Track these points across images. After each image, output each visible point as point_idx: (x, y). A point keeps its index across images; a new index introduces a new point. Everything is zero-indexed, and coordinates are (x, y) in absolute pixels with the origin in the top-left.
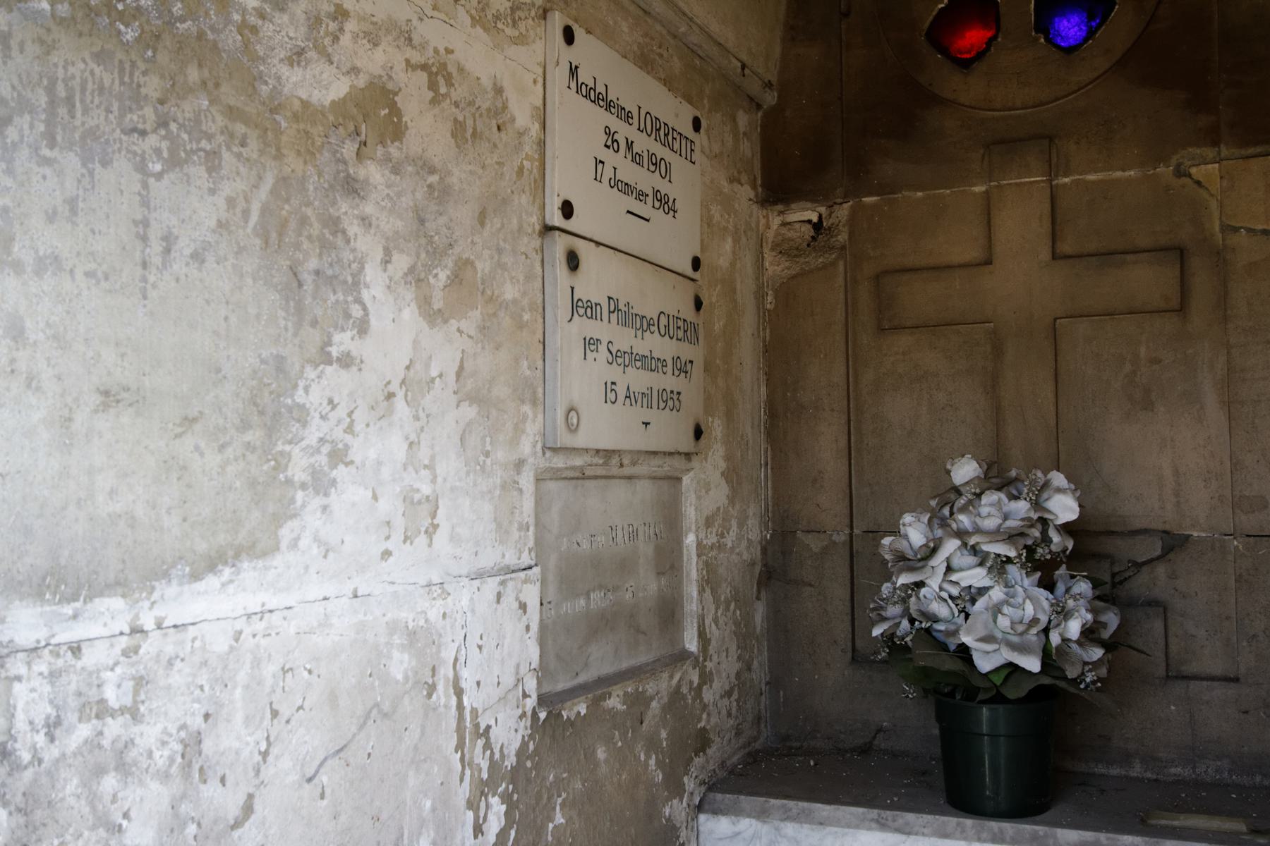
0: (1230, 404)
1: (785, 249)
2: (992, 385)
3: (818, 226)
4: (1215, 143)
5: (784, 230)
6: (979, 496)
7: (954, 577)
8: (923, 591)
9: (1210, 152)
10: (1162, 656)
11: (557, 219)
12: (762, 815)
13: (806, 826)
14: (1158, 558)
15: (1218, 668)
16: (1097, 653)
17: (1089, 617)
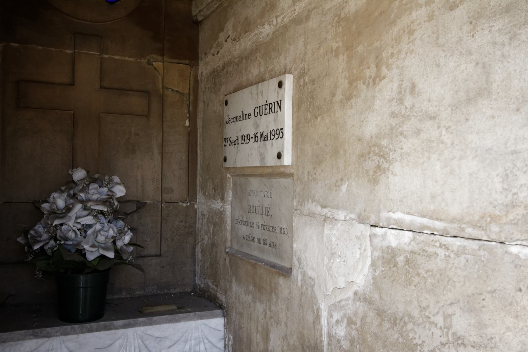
0: (162, 154)
4: (163, 55)
6: (88, 185)
8: (64, 227)
9: (160, 58)
14: (135, 211)
15: (153, 251)
16: (131, 249)
17: (132, 234)
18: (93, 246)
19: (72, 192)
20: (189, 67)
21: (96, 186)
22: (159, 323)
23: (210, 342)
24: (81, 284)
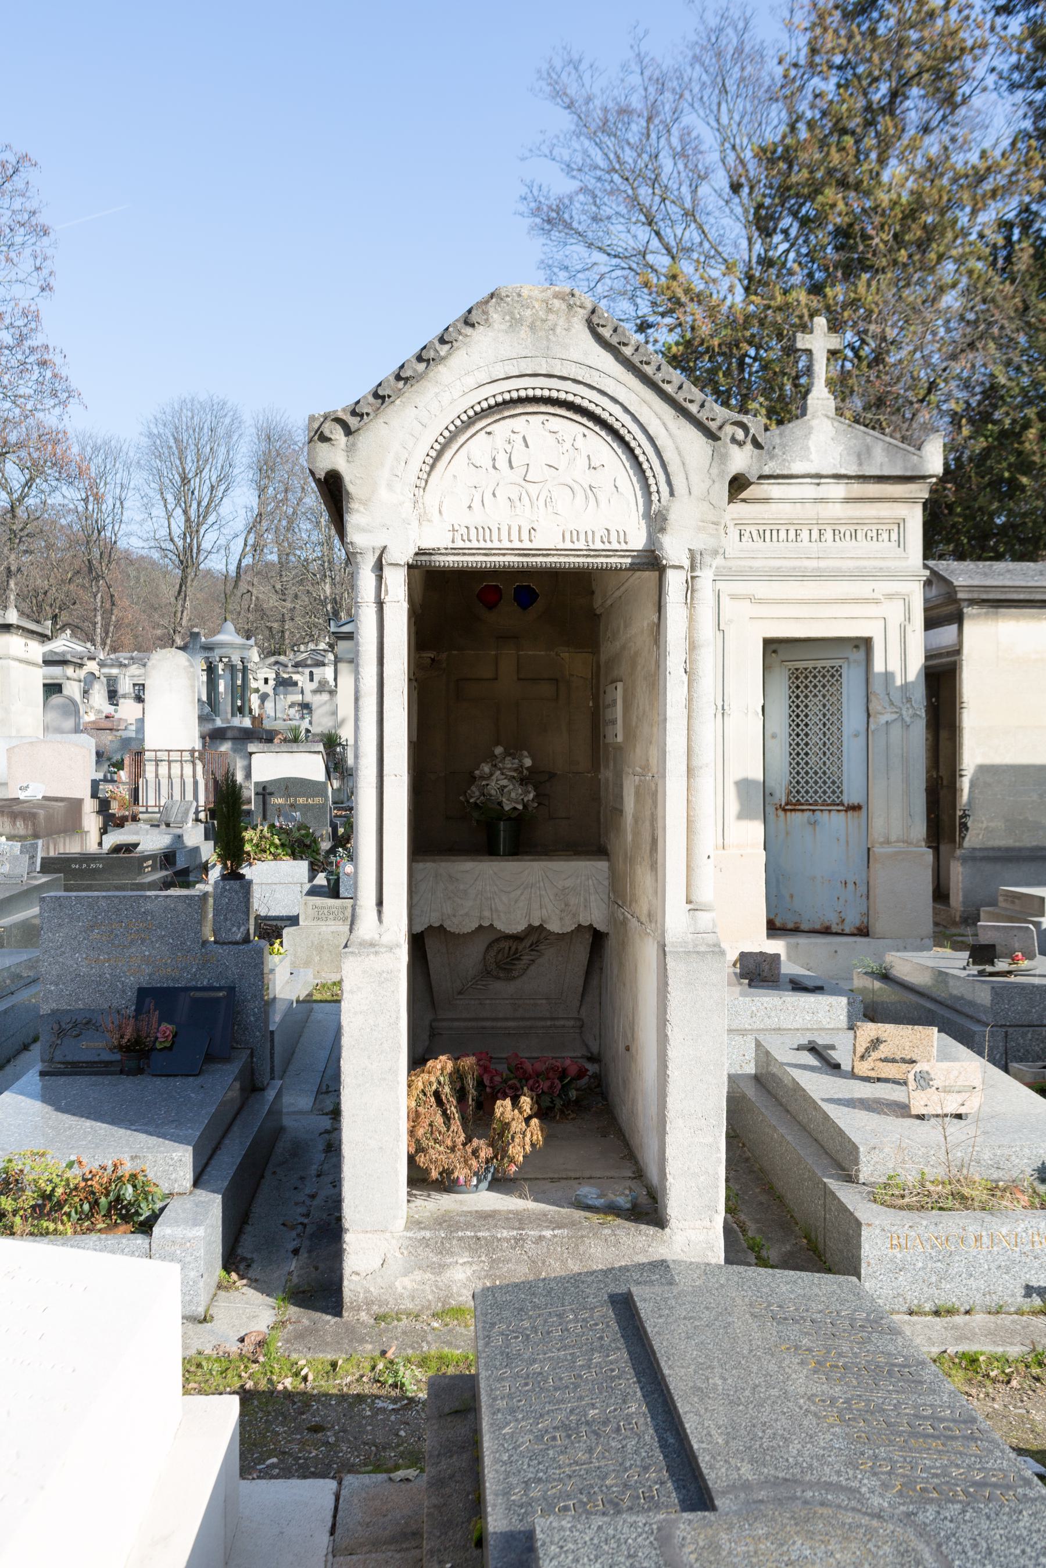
3: (433, 660)
12: (434, 861)
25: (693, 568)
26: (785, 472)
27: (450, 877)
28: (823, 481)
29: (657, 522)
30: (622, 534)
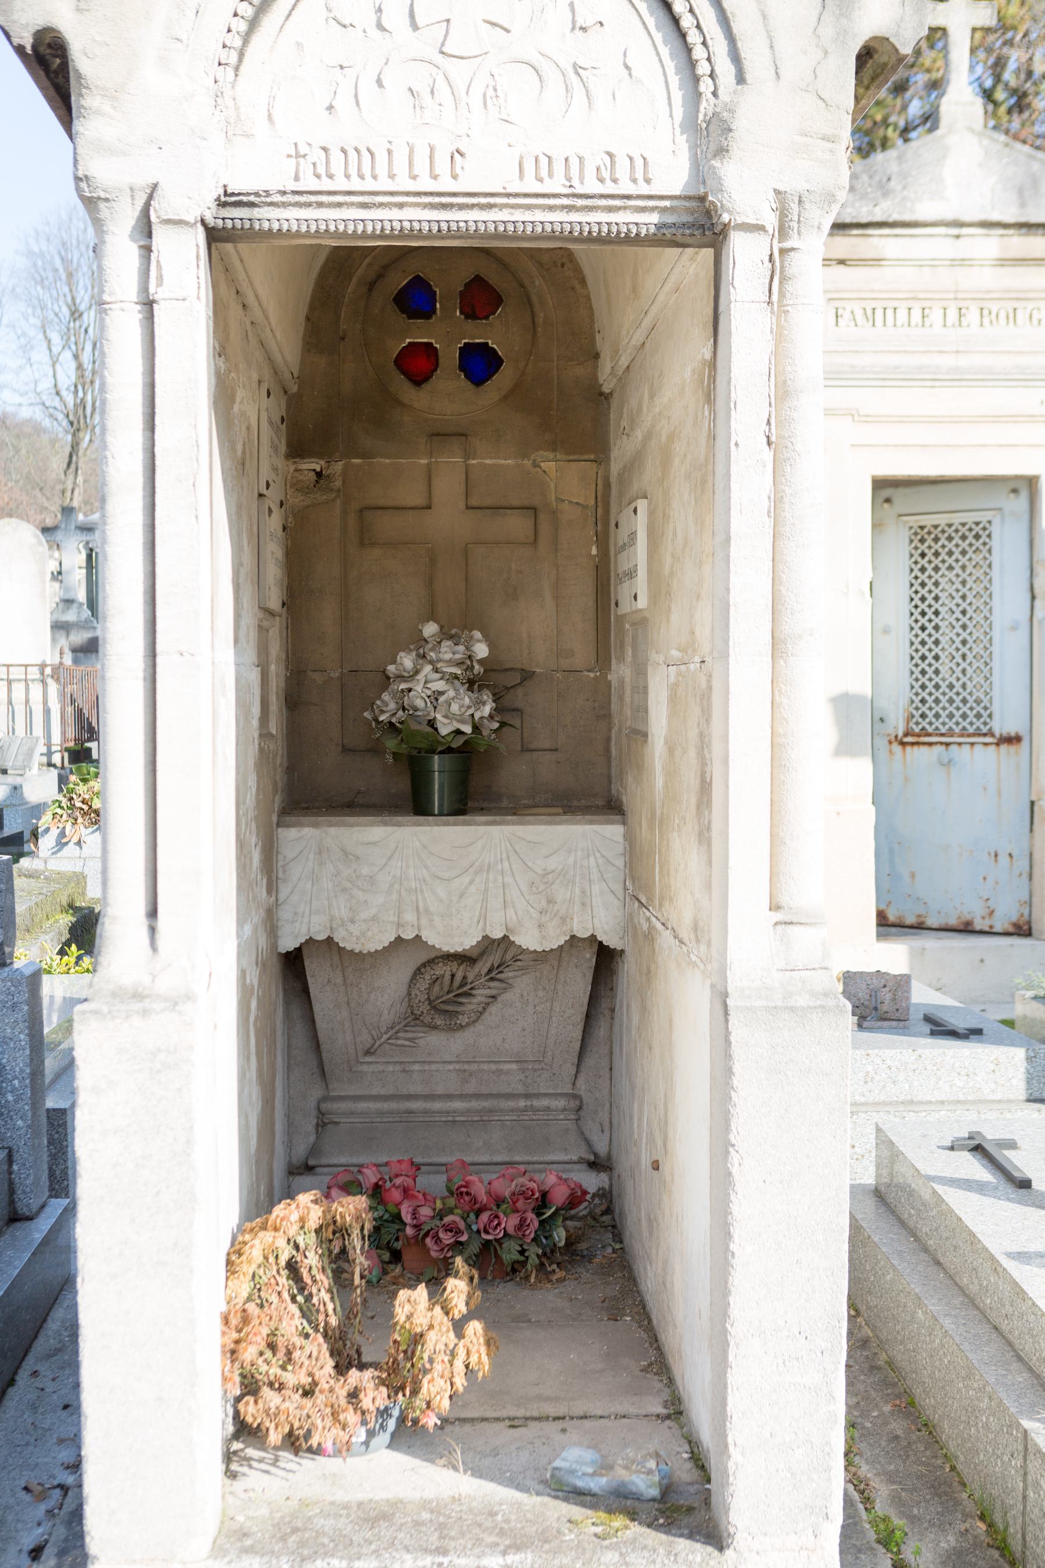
0: (557, 597)
1: (298, 486)
2: (430, 582)
3: (319, 474)
4: (554, 450)
5: (297, 474)
6: (439, 643)
7: (429, 686)
9: (551, 455)
10: (519, 739)
11: (265, 492)
12: (315, 825)
13: (342, 828)
15: (547, 745)
18: (446, 717)
19: (421, 651)
20: (595, 465)
21: (449, 643)
22: (533, 824)
23: (603, 856)
24: (436, 768)
25: (783, 231)
26: (907, 217)
27: (346, 853)
28: (965, 231)
29: (710, 137)
30: (639, 163)
